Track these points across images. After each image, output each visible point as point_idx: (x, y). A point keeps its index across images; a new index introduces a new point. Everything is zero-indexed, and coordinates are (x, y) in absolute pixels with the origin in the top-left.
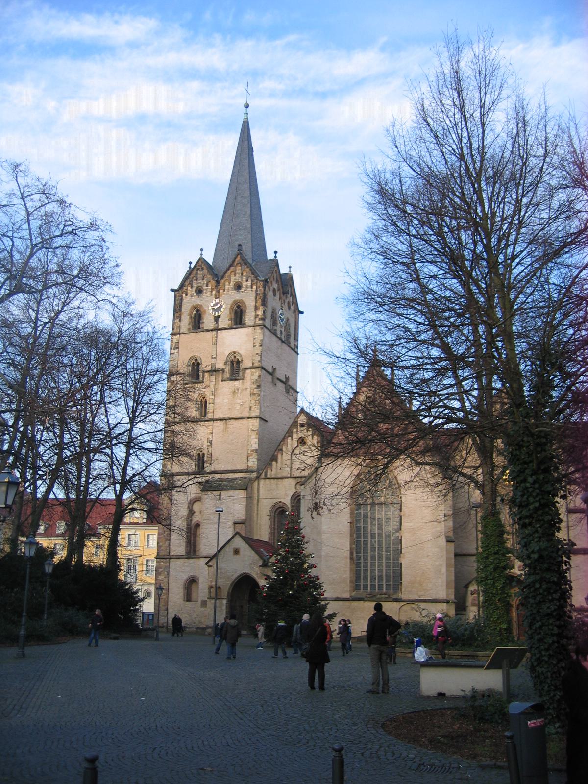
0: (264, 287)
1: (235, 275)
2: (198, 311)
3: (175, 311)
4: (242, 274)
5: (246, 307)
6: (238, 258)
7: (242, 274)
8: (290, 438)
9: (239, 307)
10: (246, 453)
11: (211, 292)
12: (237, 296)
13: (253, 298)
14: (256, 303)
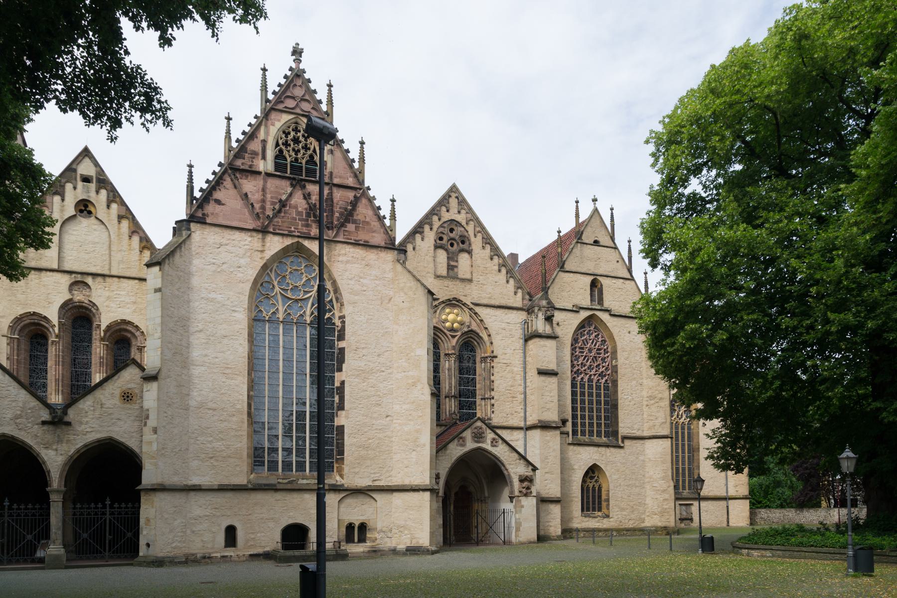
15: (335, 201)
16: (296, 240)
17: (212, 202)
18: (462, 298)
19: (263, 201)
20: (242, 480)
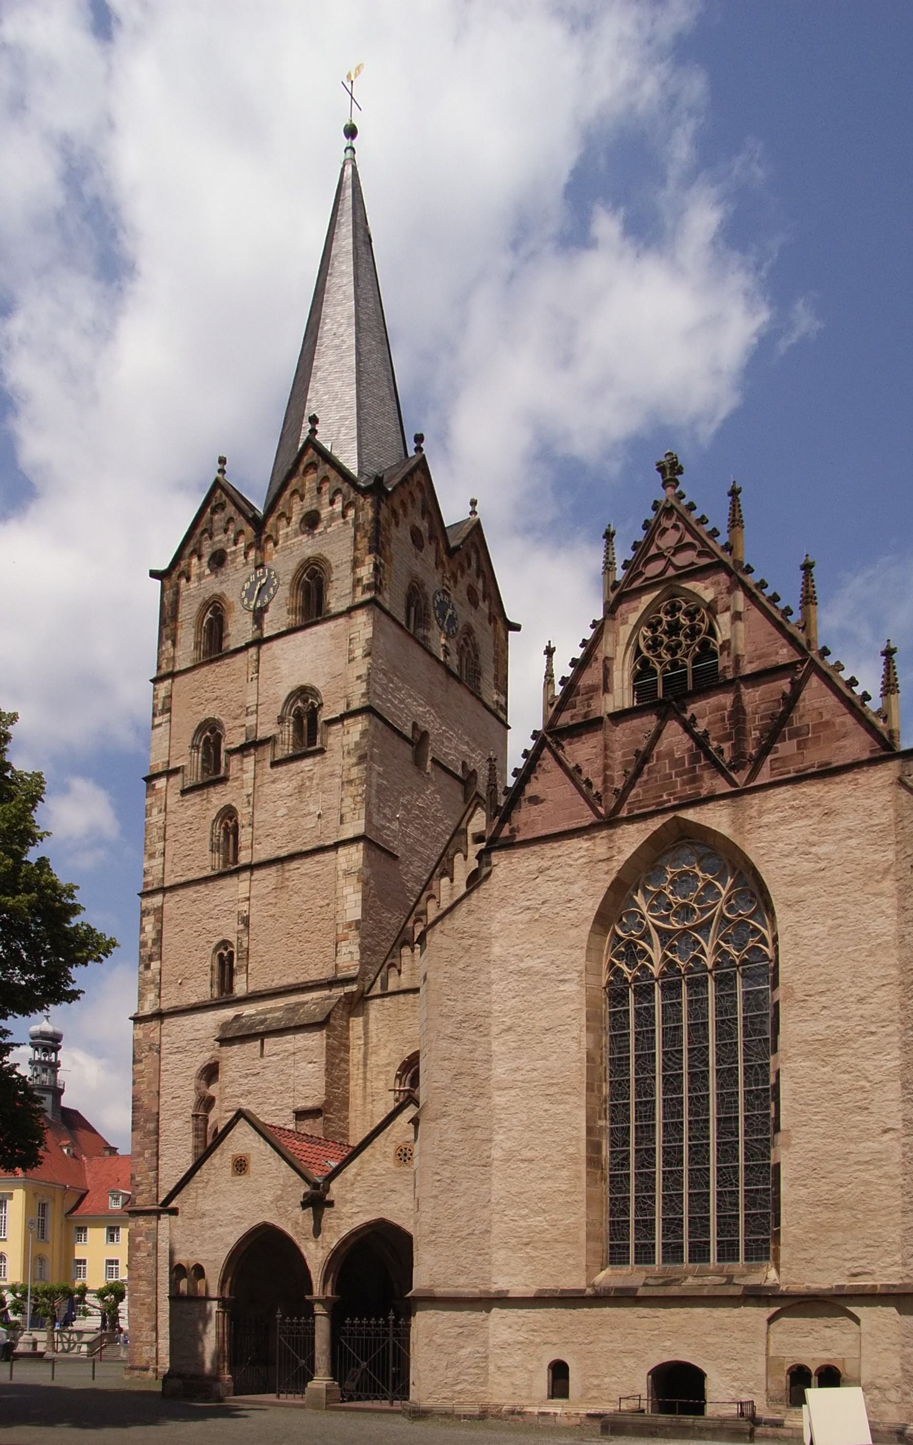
1: (302, 498)
3: (163, 623)
4: (319, 490)
7: (319, 490)
8: (445, 881)
9: (314, 575)
11: (246, 555)
13: (349, 543)
15: (749, 710)
16: (672, 815)
17: (524, 804)
19: (606, 767)
20: (575, 1281)
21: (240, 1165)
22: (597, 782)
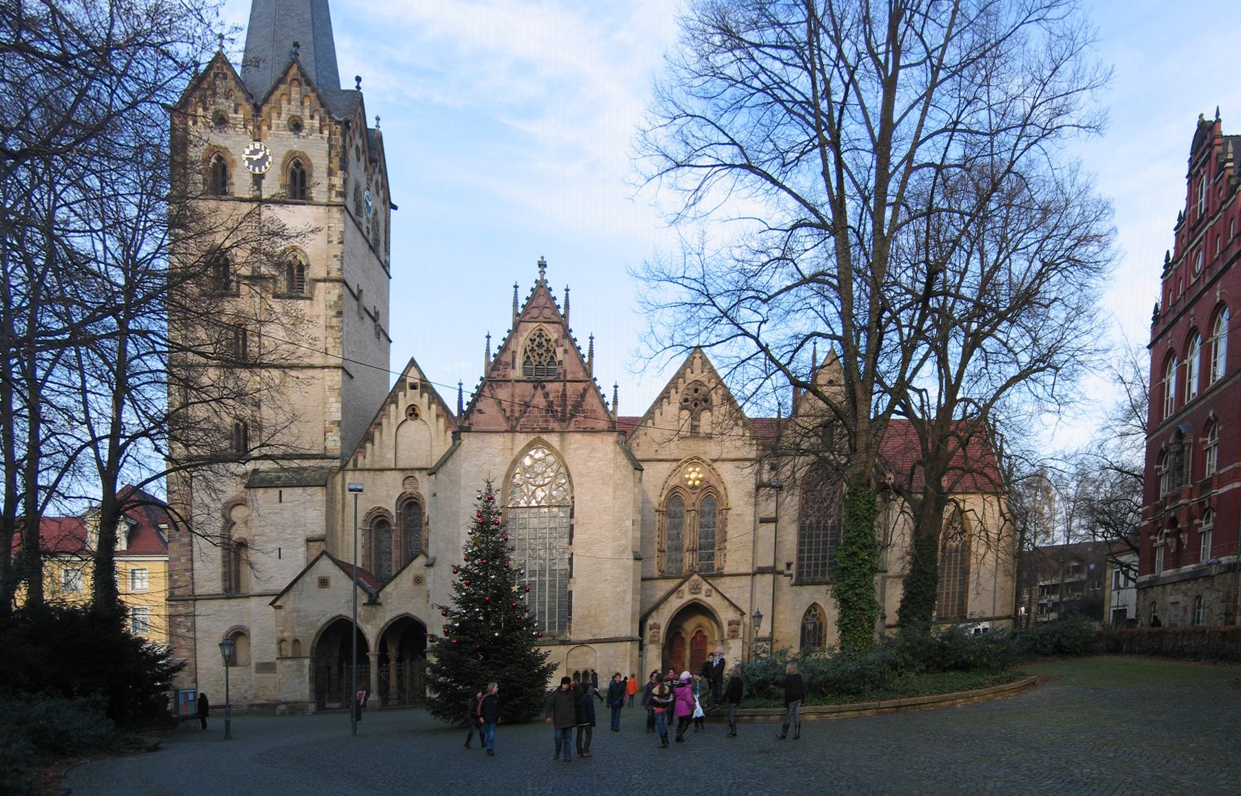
0: (343, 135)
1: (289, 102)
2: (219, 159)
5: (311, 166)
6: (294, 70)
7: (302, 103)
9: (298, 164)
10: (321, 427)
12: (295, 143)
13: (325, 154)
14: (330, 162)
18: (702, 456)
21: (324, 582)
22: (508, 410)
